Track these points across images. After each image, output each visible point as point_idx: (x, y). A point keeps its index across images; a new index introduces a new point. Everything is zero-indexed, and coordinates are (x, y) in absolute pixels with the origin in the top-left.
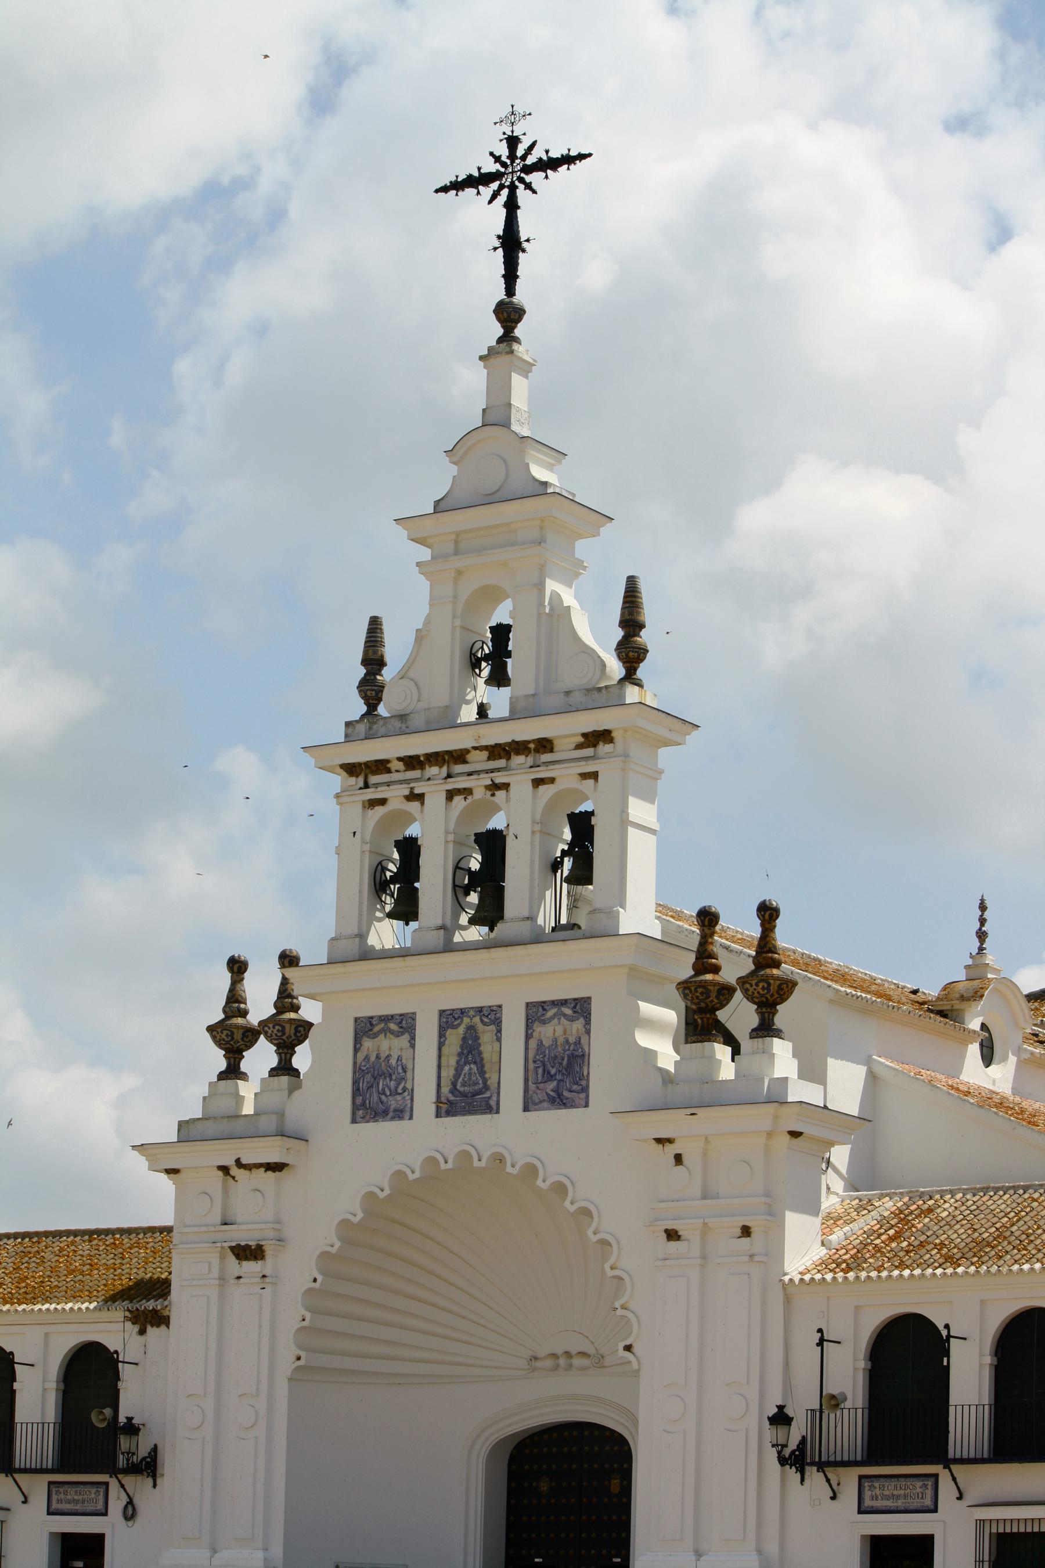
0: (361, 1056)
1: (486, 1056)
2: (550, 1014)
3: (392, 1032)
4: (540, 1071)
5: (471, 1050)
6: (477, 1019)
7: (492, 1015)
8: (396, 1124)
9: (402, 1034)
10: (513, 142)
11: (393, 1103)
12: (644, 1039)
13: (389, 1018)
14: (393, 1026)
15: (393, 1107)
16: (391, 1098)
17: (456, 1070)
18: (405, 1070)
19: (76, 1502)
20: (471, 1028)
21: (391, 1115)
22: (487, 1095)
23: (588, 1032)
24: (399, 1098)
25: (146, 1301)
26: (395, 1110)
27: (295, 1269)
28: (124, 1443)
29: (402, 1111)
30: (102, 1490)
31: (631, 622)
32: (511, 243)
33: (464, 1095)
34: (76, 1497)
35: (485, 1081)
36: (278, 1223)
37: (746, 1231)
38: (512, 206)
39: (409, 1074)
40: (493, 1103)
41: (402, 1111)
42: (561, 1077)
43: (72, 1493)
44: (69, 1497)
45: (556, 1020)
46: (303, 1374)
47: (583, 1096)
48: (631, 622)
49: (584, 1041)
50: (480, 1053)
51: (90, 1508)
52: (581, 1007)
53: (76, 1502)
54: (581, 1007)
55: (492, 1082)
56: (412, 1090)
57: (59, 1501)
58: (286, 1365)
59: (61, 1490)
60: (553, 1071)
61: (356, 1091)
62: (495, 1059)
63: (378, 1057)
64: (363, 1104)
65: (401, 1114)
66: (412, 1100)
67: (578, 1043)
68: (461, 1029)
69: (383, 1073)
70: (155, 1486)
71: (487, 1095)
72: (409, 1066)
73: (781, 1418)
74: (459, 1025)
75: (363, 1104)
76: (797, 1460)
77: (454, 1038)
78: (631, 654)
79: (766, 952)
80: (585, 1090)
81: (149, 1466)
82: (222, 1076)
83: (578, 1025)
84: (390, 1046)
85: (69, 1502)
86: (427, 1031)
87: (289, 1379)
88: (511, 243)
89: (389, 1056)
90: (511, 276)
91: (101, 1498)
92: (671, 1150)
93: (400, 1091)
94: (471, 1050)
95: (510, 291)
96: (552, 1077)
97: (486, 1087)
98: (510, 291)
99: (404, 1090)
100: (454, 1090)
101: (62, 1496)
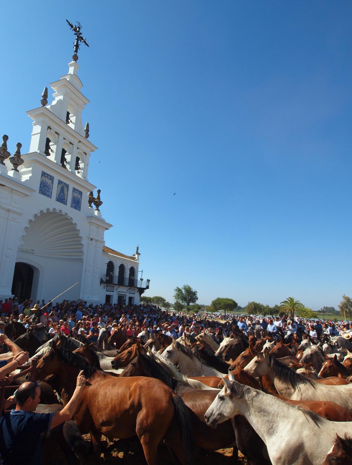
0: (42, 180)
1: (65, 193)
2: (76, 191)
3: (49, 178)
4: (73, 201)
5: (62, 190)
6: (64, 185)
8: (47, 197)
9: (50, 180)
11: (47, 193)
13: (49, 175)
14: (49, 177)
15: (47, 194)
16: (47, 192)
17: (60, 193)
18: (50, 188)
20: (63, 186)
21: (46, 195)
22: (64, 201)
23: (81, 198)
24: (49, 193)
26: (47, 195)
29: (49, 196)
31: (87, 131)
33: (60, 199)
35: (64, 198)
39: (51, 189)
40: (65, 202)
41: (49, 196)
42: (77, 204)
45: (76, 193)
47: (79, 209)
49: (80, 199)
50: (64, 192)
55: (66, 198)
56: (51, 193)
60: (75, 202)
61: (40, 186)
62: (67, 194)
63: (45, 181)
64: (41, 190)
65: (48, 196)
66: (51, 194)
67: (79, 199)
68: (61, 185)
69: (46, 186)
71: (64, 201)
72: (51, 187)
74: (61, 184)
75: (41, 190)
77: (60, 186)
80: (80, 208)
83: (79, 196)
86: (56, 182)
89: (47, 183)
90: (76, 51)
93: (49, 191)
96: (75, 203)
97: (64, 199)
99: (50, 192)
100: (59, 197)
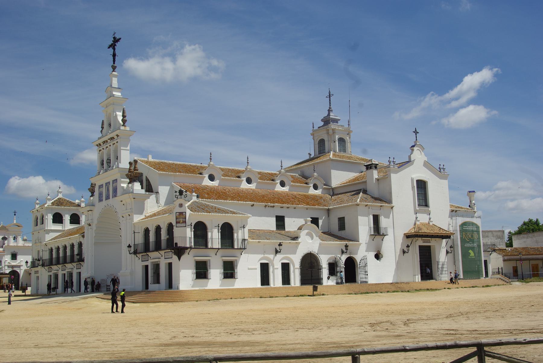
7: (109, 183)
10: (114, 38)
12: (122, 185)
32: (114, 55)
37: (129, 215)
38: (114, 49)
46: (96, 244)
48: (124, 116)
52: (116, 180)
54: (116, 180)
73: (129, 246)
76: (135, 253)
78: (124, 121)
79: (135, 169)
81: (83, 261)
82: (91, 196)
84: (101, 189)
88: (114, 55)
92: (122, 203)
94: (108, 190)
95: (114, 63)
98: (114, 63)
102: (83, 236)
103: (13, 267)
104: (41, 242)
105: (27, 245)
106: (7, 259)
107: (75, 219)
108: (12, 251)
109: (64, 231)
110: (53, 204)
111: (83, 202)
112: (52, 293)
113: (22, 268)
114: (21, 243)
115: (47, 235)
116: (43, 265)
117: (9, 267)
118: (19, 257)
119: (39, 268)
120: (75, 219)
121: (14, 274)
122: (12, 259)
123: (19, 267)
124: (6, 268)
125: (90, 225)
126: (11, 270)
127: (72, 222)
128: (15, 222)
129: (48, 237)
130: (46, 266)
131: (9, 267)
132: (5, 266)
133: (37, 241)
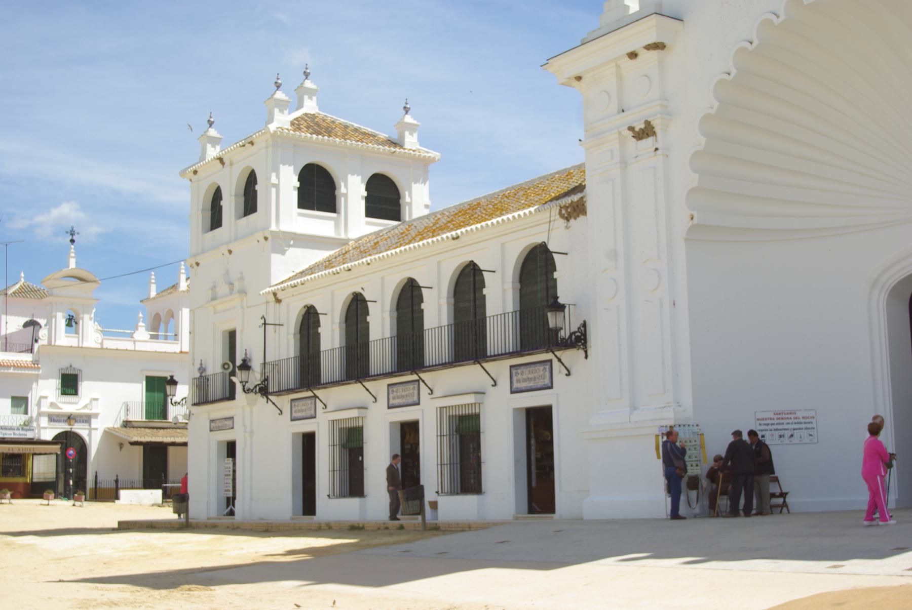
19: (529, 379)
25: (572, 202)
27: (682, 136)
28: (551, 317)
30: (548, 367)
34: (530, 376)
36: (666, 100)
43: (526, 373)
44: (525, 377)
46: (699, 233)
51: (540, 383)
53: (529, 379)
57: (518, 381)
58: (682, 225)
59: (519, 371)
70: (586, 357)
81: (579, 340)
85: (525, 380)
87: (686, 240)
91: (548, 374)
101: (520, 376)
102: (577, 210)
103: (70, 418)
104: (243, 292)
105: (110, 344)
106: (47, 390)
107: (384, 198)
108: (64, 364)
109: (345, 242)
110: (296, 124)
111: (412, 128)
112: (404, 520)
113: (95, 423)
114: (91, 334)
115: (275, 258)
116: (264, 390)
117: (53, 418)
118: (84, 386)
119: (244, 407)
120: (384, 198)
121: (71, 446)
122: (64, 393)
123: (87, 419)
124: (44, 421)
125: (646, 132)
126: (63, 427)
127: (371, 212)
128: (72, 264)
129: (285, 266)
130: (279, 393)
131: (53, 418)
132: (40, 414)
133: (223, 289)
